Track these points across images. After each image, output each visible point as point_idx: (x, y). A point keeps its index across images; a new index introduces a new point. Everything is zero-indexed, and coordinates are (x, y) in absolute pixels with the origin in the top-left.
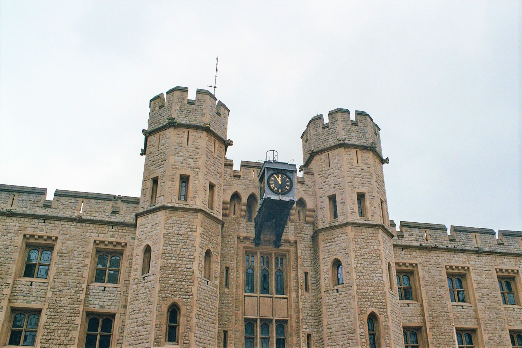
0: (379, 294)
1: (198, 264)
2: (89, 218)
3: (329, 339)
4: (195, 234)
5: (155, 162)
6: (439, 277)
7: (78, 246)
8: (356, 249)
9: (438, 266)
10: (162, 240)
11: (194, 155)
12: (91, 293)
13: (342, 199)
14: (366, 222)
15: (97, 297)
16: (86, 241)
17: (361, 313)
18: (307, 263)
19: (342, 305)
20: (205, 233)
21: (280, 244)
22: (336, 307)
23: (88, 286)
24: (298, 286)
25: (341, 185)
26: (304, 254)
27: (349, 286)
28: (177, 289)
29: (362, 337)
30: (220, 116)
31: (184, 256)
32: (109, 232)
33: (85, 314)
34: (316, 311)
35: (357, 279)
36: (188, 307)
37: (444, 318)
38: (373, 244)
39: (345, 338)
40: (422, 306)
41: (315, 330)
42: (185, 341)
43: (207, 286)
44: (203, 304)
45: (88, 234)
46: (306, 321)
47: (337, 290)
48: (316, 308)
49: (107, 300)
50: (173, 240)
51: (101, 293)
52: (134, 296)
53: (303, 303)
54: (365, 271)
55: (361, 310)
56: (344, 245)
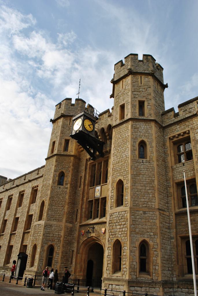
43: (59, 190)
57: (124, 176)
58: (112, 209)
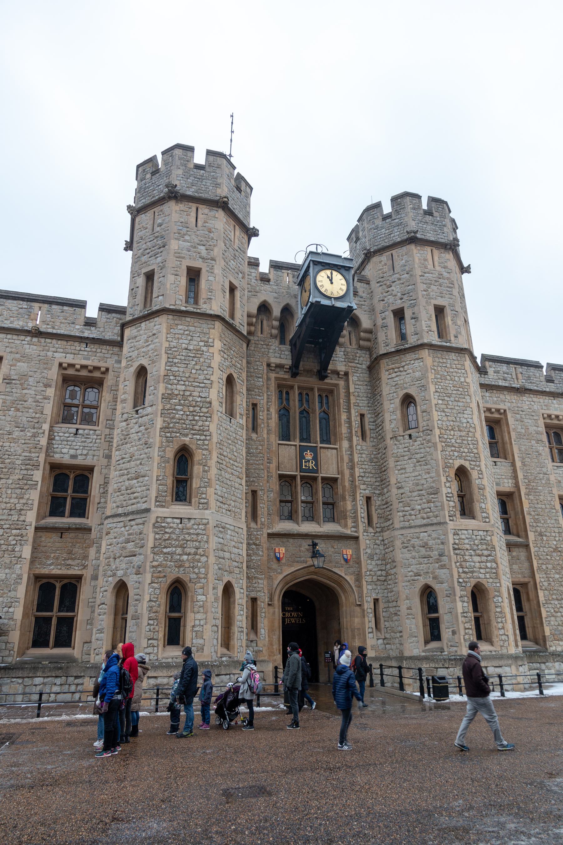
0: (470, 442)
1: (217, 392)
2: (50, 330)
3: (399, 502)
4: (211, 350)
5: (148, 251)
6: (535, 428)
7: (36, 370)
8: (436, 380)
9: (533, 414)
10: (164, 357)
11: (207, 241)
12: (57, 438)
13: (414, 313)
14: (448, 344)
15: (66, 443)
16: (47, 364)
17: (447, 466)
18: (363, 402)
19: (418, 456)
20: (226, 351)
21: (325, 374)
22: (409, 459)
23: (51, 427)
24: (351, 433)
25: (411, 294)
26: (358, 390)
27: (427, 430)
28: (188, 426)
29: (449, 499)
30: (240, 193)
31: (196, 380)
32: (81, 352)
33: (48, 467)
34: (377, 467)
35: (439, 420)
36: (205, 452)
37: (544, 482)
38: (459, 375)
39: (425, 500)
40: (513, 464)
41: (377, 492)
42: (202, 501)
44: (224, 448)
45: (50, 354)
46: (364, 479)
47: (410, 436)
48: (377, 462)
49: (81, 448)
50: (178, 357)
51: (72, 437)
52: (123, 437)
53: (359, 455)
54: (450, 411)
55: (446, 463)
56: (418, 374)
57: (472, 463)
58: (453, 520)
